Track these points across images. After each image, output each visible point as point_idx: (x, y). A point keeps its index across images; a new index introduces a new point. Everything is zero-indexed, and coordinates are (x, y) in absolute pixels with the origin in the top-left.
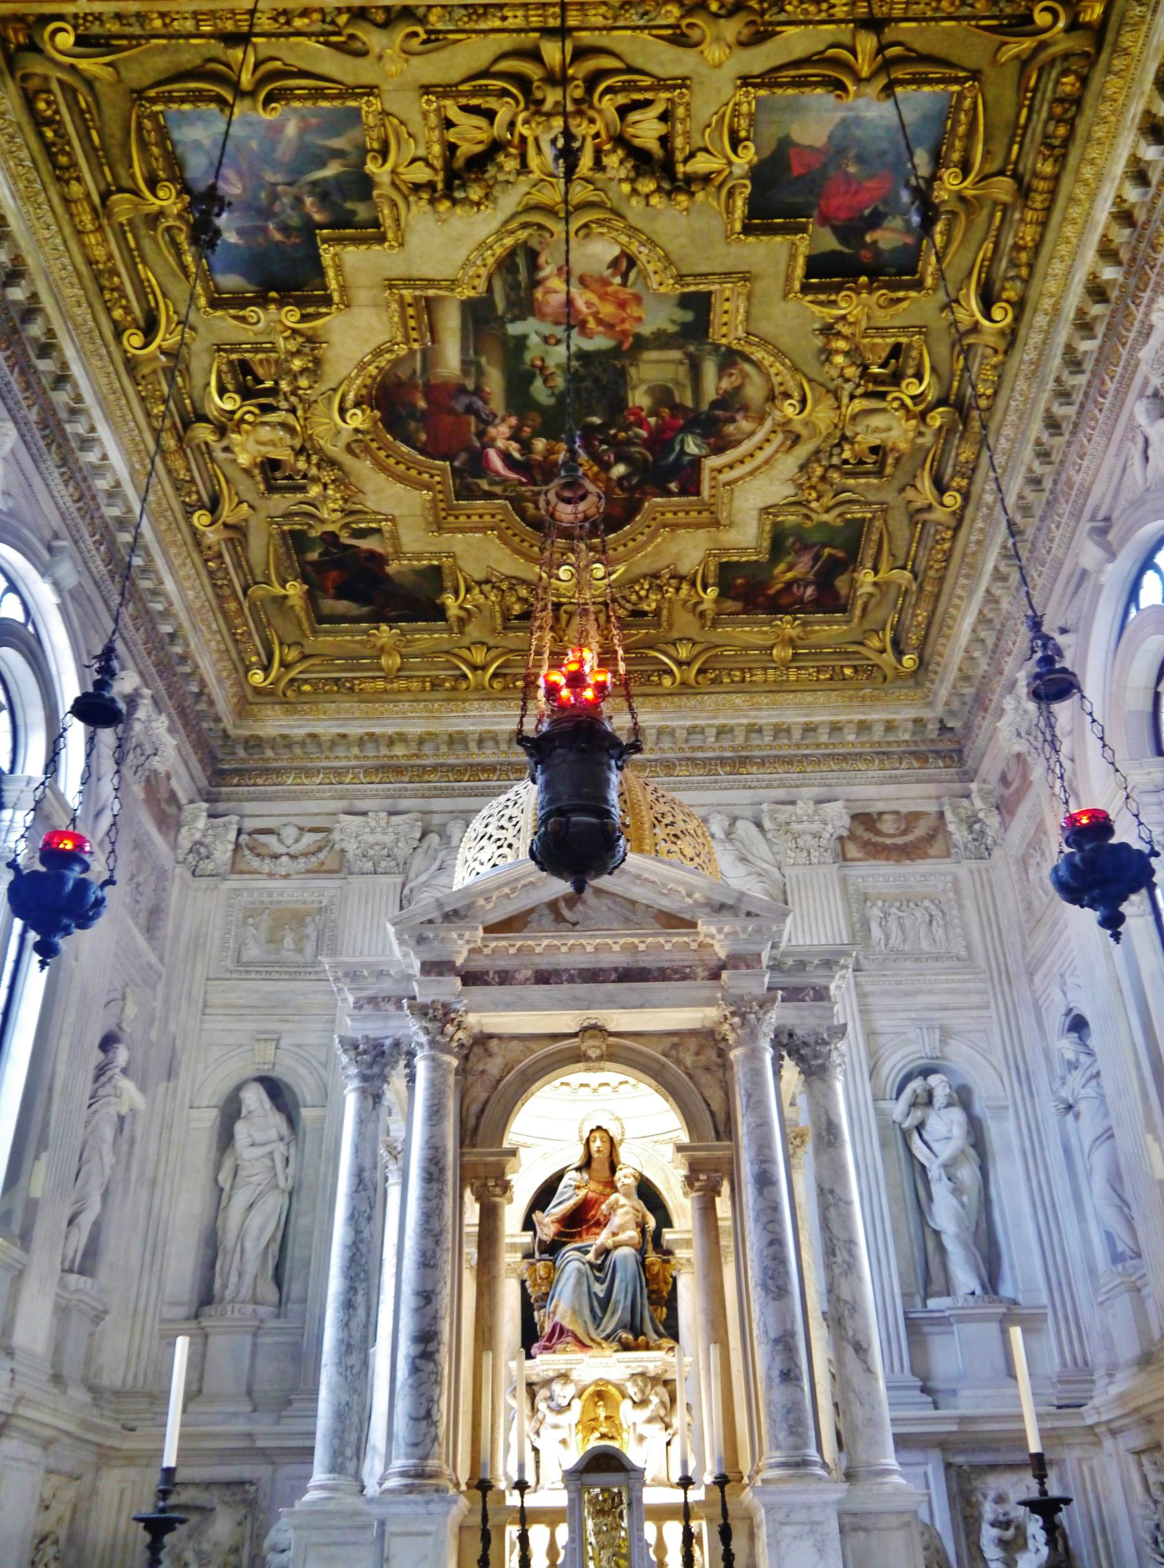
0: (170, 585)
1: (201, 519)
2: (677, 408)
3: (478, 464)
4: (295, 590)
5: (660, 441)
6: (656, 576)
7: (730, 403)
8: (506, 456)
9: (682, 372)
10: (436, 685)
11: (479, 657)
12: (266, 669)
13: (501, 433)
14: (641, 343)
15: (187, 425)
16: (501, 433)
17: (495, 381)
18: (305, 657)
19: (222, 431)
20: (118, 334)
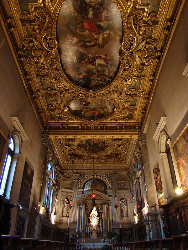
0: (59, 157)
1: (63, 153)
2: (103, 146)
3: (86, 149)
4: (69, 156)
5: (101, 148)
6: (101, 156)
7: (108, 146)
8: (88, 148)
9: (103, 144)
10: (81, 162)
11: (85, 160)
12: (66, 161)
13: (88, 147)
14: (100, 143)
15: (62, 147)
16: (88, 147)
17: (88, 144)
18: (70, 160)
19: (65, 148)
20: (58, 143)
